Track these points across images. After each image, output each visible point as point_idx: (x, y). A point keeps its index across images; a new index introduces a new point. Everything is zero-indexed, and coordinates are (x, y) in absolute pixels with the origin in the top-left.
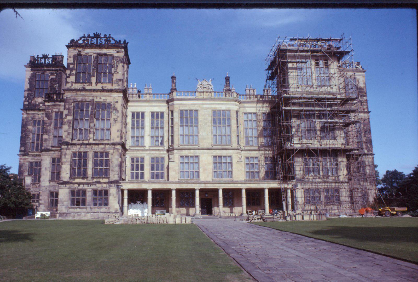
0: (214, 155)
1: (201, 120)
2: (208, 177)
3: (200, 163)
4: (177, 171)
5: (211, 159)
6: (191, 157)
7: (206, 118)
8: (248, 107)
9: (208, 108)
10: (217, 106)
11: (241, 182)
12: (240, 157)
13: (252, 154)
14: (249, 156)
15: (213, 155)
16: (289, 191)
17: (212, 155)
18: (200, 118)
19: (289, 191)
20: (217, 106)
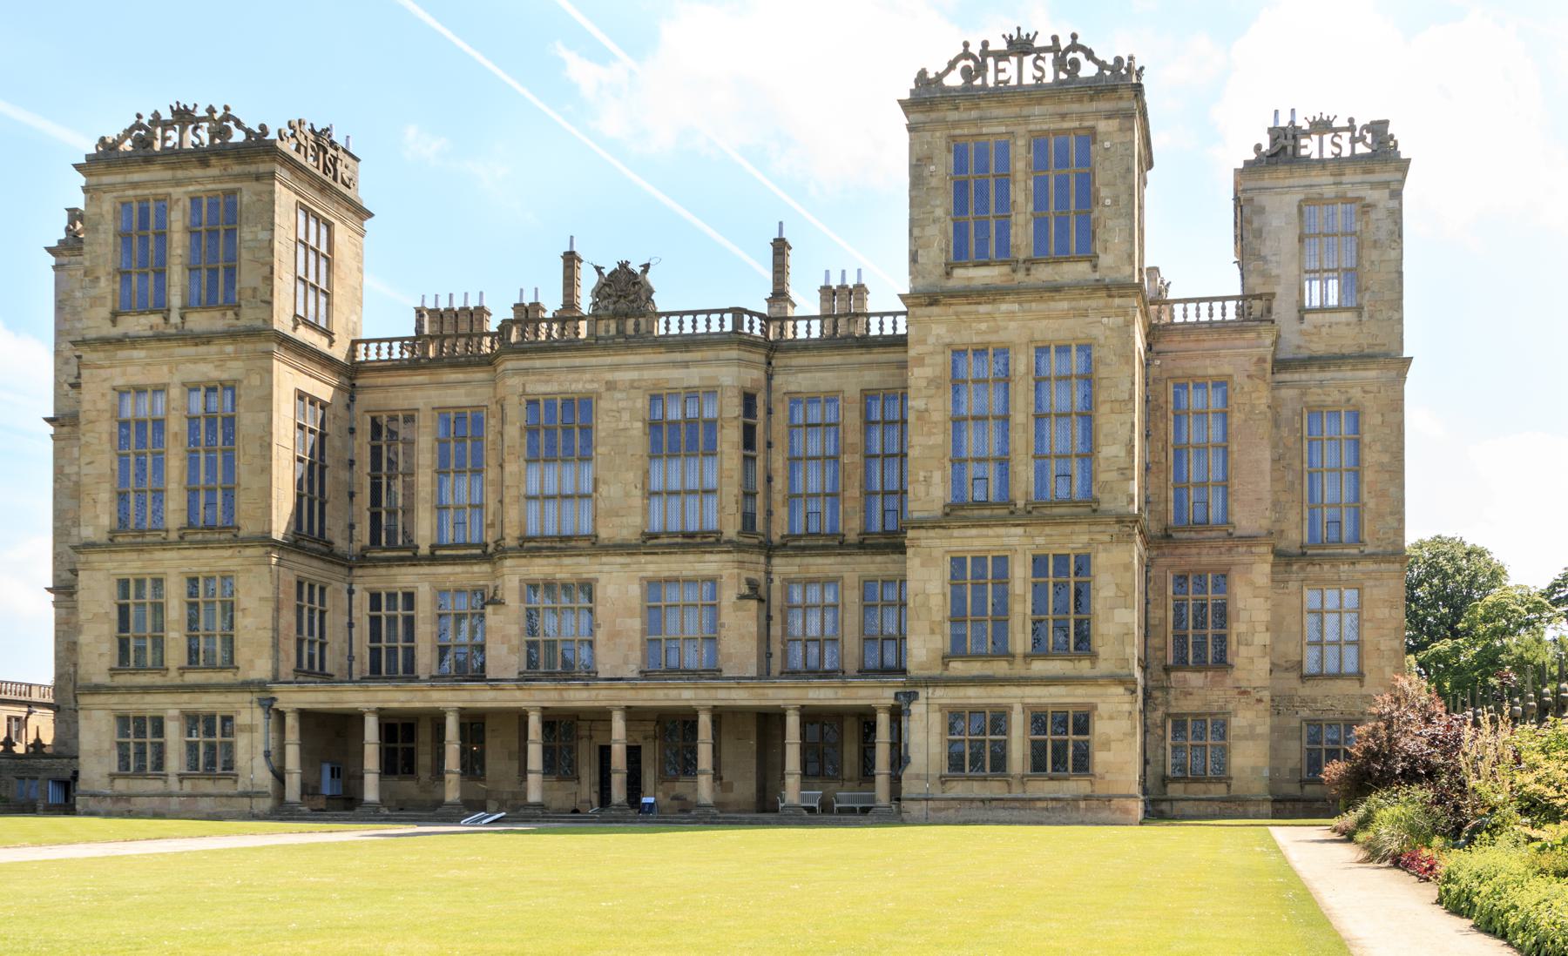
0: (650, 574)
1: (603, 434)
2: (626, 663)
3: (599, 610)
4: (515, 642)
5: (635, 590)
6: (566, 587)
7: (621, 426)
8: (802, 369)
9: (633, 385)
10: (665, 373)
11: (739, 680)
12: (759, 576)
13: (813, 569)
14: (798, 576)
15: (644, 574)
16: (883, 720)
17: (641, 574)
18: (603, 426)
19: (883, 720)
20: (665, 373)
